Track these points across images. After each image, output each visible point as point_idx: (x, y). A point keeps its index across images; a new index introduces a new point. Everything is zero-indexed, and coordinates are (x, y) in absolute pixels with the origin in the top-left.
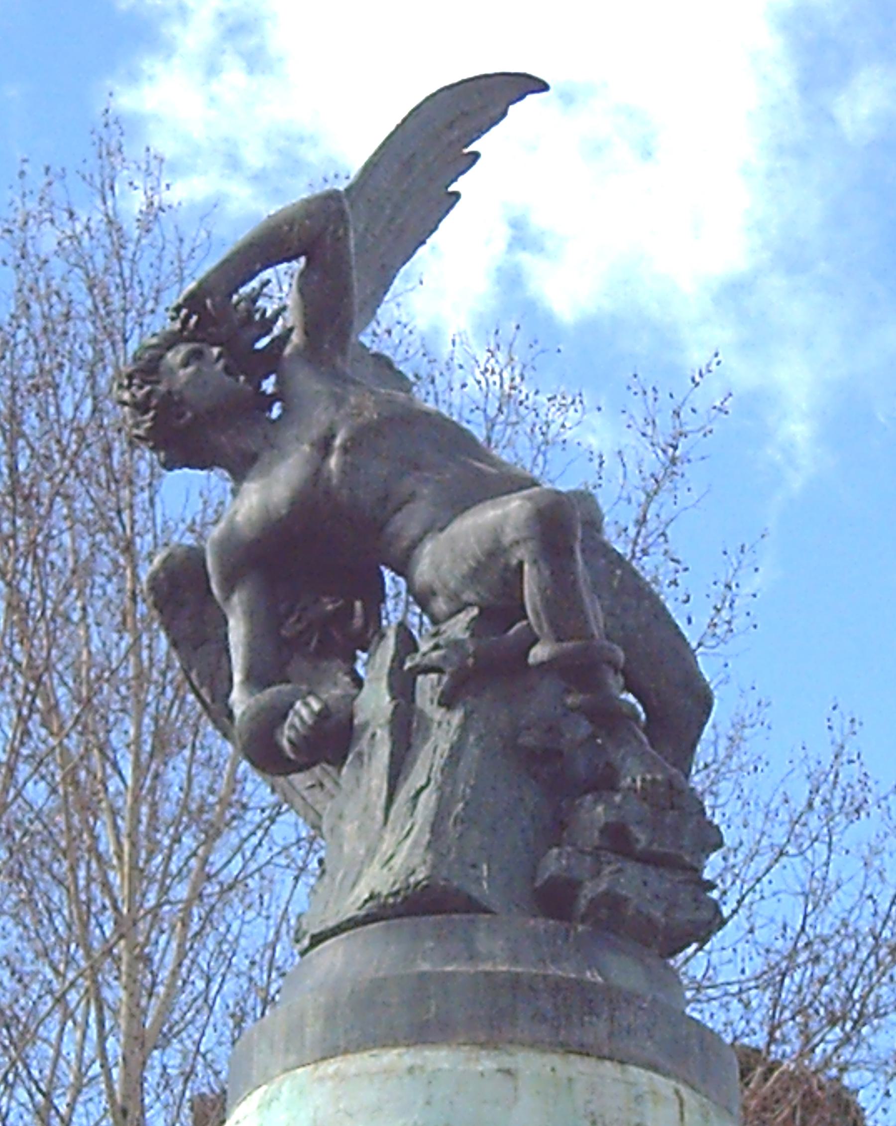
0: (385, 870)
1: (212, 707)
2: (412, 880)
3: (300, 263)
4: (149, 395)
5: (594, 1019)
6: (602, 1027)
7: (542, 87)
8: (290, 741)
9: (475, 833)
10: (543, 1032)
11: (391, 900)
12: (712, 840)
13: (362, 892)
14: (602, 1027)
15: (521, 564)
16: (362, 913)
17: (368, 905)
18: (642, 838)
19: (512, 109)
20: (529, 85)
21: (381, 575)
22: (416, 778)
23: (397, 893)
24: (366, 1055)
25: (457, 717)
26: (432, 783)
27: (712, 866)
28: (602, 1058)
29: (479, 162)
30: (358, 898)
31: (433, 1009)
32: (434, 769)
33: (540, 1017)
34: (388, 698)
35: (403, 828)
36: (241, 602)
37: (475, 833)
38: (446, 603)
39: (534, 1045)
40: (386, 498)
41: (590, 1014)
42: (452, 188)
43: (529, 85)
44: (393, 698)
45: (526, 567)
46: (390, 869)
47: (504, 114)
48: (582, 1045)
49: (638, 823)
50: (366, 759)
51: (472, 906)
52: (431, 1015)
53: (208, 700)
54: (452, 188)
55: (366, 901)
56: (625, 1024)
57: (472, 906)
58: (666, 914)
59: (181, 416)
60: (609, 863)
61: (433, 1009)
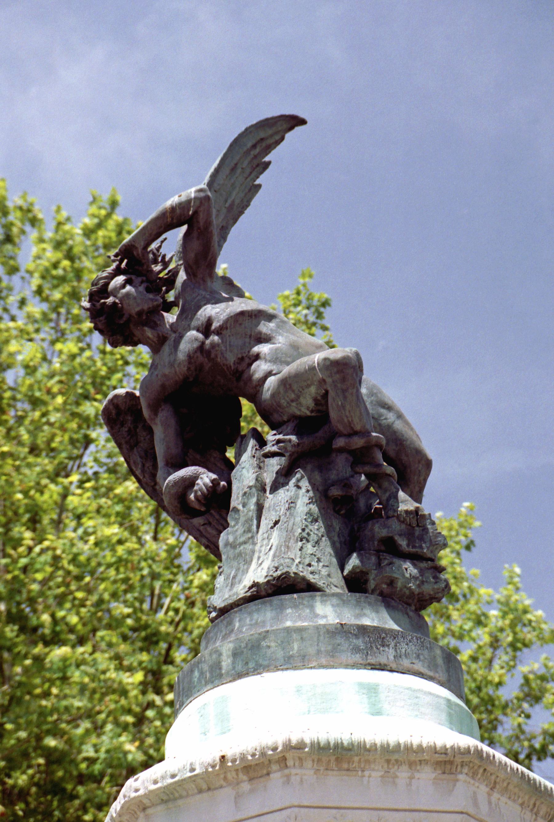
0: (260, 569)
5: (386, 649)
6: (391, 653)
7: (303, 122)
9: (309, 546)
10: (357, 658)
13: (247, 581)
14: (391, 653)
16: (249, 594)
17: (251, 590)
18: (403, 543)
19: (288, 136)
20: (295, 121)
21: (239, 402)
23: (268, 581)
28: (392, 671)
29: (271, 167)
30: (245, 586)
33: (356, 650)
37: (309, 546)
39: (355, 666)
40: (242, 359)
41: (383, 646)
42: (257, 182)
43: (295, 121)
47: (282, 139)
48: (380, 664)
49: (400, 535)
51: (311, 588)
54: (257, 182)
55: (250, 588)
56: (403, 650)
57: (311, 588)
58: (419, 586)
59: (122, 316)
60: (385, 559)
61: (296, 646)
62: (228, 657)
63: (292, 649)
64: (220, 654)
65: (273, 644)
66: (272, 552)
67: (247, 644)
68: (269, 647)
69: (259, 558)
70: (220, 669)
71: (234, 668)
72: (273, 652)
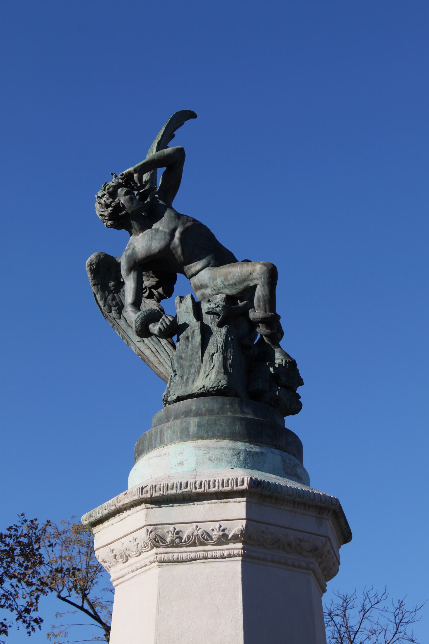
1: (102, 308)
2: (220, 384)
3: (165, 168)
4: (111, 202)
8: (160, 329)
11: (212, 389)
12: (300, 382)
15: (255, 286)
16: (199, 392)
17: (202, 390)
20: (193, 115)
22: (211, 348)
23: (214, 387)
24: (215, 440)
25: (224, 330)
26: (219, 351)
27: (300, 390)
31: (237, 428)
32: (218, 347)
34: (195, 320)
35: (210, 366)
36: (133, 277)
38: (212, 291)
44: (198, 321)
45: (258, 287)
46: (210, 379)
50: (190, 339)
52: (237, 431)
53: (102, 305)
55: (201, 388)
61: (237, 428)
62: (195, 426)
63: (235, 429)
64: (189, 424)
65: (224, 424)
66: (214, 370)
67: (208, 421)
68: (222, 425)
69: (205, 371)
70: (189, 432)
71: (198, 433)
72: (224, 429)
